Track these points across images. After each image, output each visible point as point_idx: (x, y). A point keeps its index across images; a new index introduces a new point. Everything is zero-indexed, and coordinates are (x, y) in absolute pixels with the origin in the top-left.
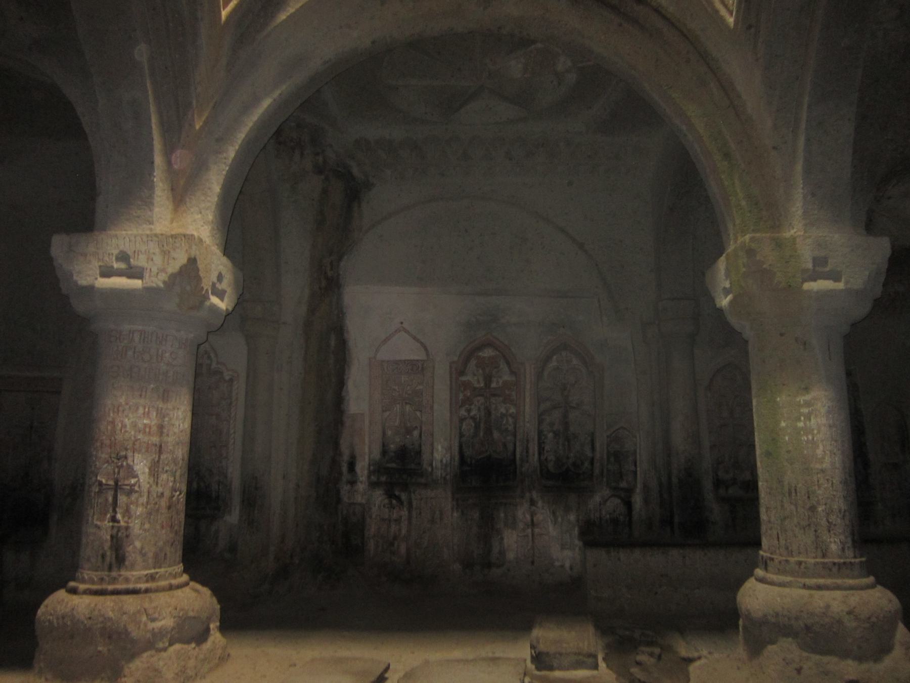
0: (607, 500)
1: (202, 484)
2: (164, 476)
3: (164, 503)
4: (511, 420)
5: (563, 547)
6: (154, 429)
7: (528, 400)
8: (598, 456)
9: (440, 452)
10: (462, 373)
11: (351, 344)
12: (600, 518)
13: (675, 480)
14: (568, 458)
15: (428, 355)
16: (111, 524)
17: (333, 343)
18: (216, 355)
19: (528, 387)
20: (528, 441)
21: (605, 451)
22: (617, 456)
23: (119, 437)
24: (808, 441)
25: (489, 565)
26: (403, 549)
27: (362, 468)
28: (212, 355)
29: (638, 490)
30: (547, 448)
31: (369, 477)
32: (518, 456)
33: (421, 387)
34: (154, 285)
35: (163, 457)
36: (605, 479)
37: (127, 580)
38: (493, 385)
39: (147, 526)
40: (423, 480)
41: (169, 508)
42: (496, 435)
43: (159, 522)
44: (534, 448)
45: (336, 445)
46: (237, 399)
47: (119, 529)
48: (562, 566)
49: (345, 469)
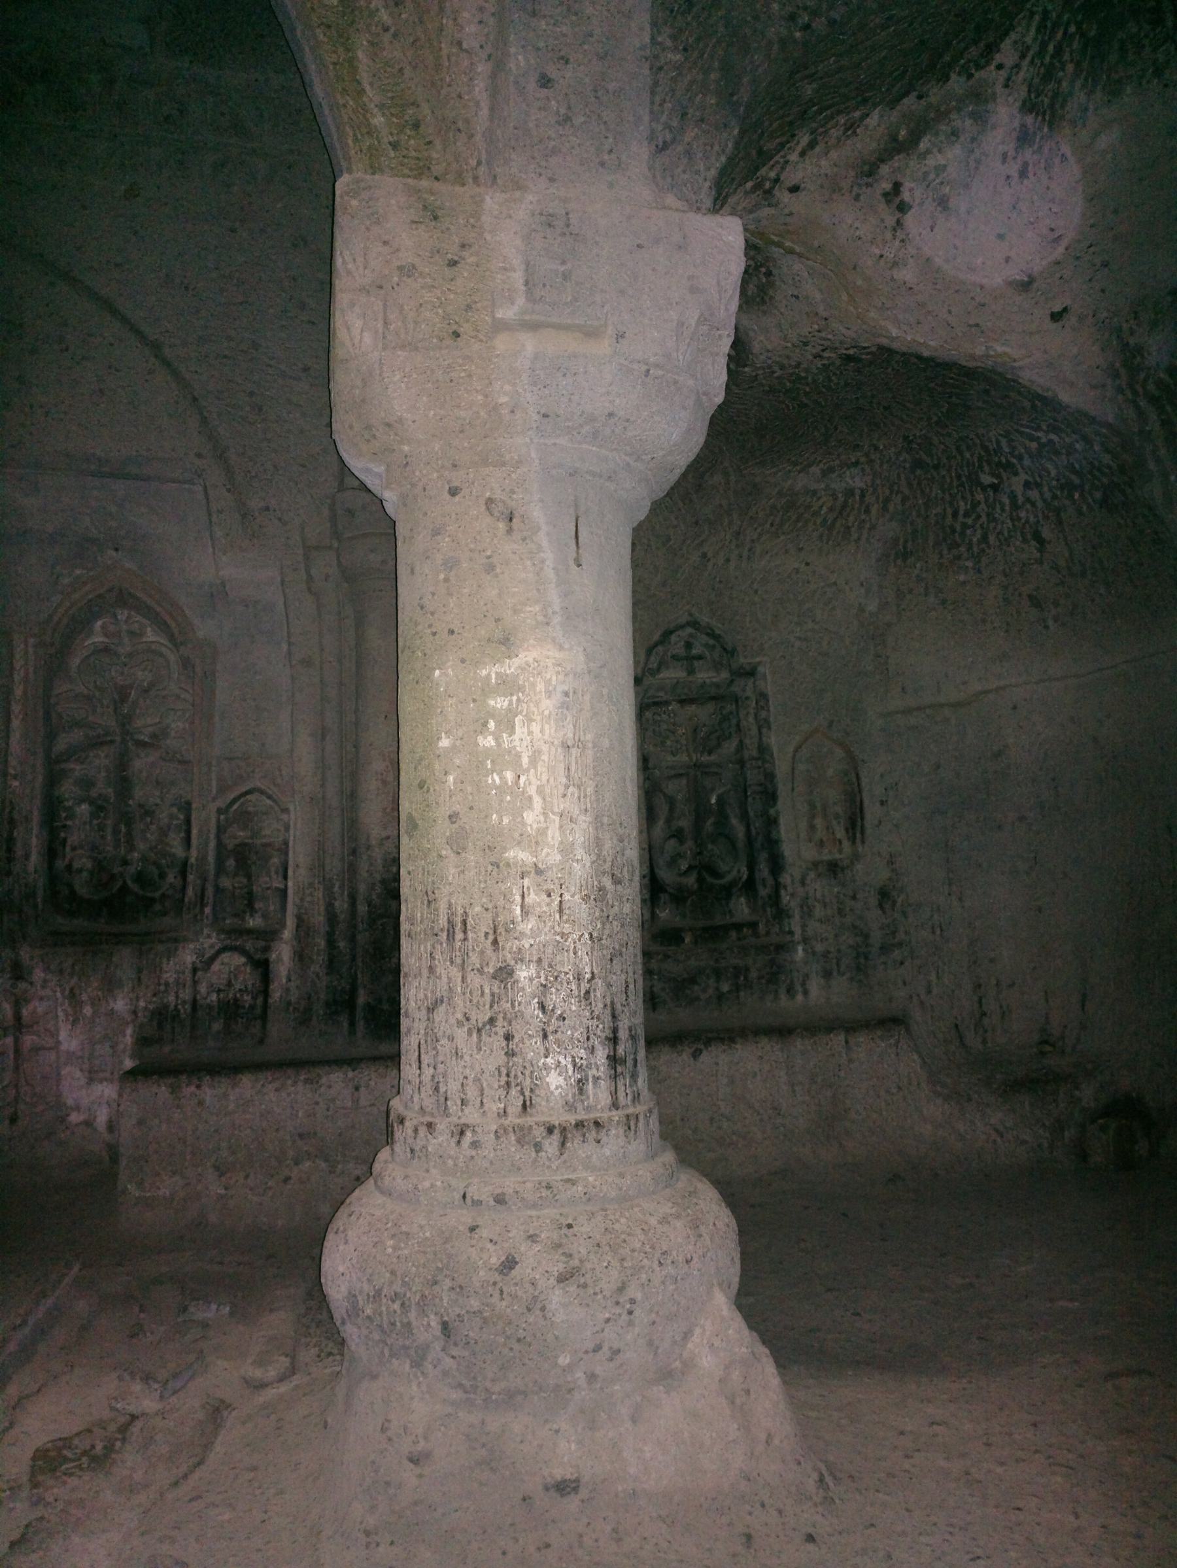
0: (213, 959)
5: (92, 1077)
7: (16, 723)
8: (194, 853)
12: (195, 1001)
13: (362, 908)
14: (125, 863)
19: (18, 692)
20: (12, 821)
21: (212, 844)
22: (243, 858)
24: (502, 789)
29: (287, 934)
30: (74, 839)
36: (207, 910)
48: (88, 1123)
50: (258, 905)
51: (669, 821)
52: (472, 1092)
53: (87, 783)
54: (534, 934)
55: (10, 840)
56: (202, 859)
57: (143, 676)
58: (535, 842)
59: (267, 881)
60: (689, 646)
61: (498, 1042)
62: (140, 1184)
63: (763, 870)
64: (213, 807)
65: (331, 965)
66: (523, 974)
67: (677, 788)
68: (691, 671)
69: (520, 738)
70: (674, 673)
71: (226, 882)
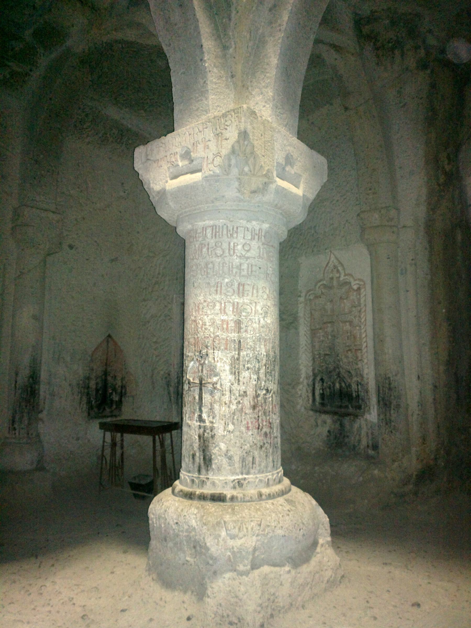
1: (343, 385)
2: (246, 374)
3: (247, 402)
6: (232, 324)
16: (198, 424)
18: (344, 269)
28: (340, 268)
34: (211, 173)
35: (243, 353)
37: (214, 484)
39: (231, 427)
41: (254, 407)
43: (244, 422)
46: (365, 305)
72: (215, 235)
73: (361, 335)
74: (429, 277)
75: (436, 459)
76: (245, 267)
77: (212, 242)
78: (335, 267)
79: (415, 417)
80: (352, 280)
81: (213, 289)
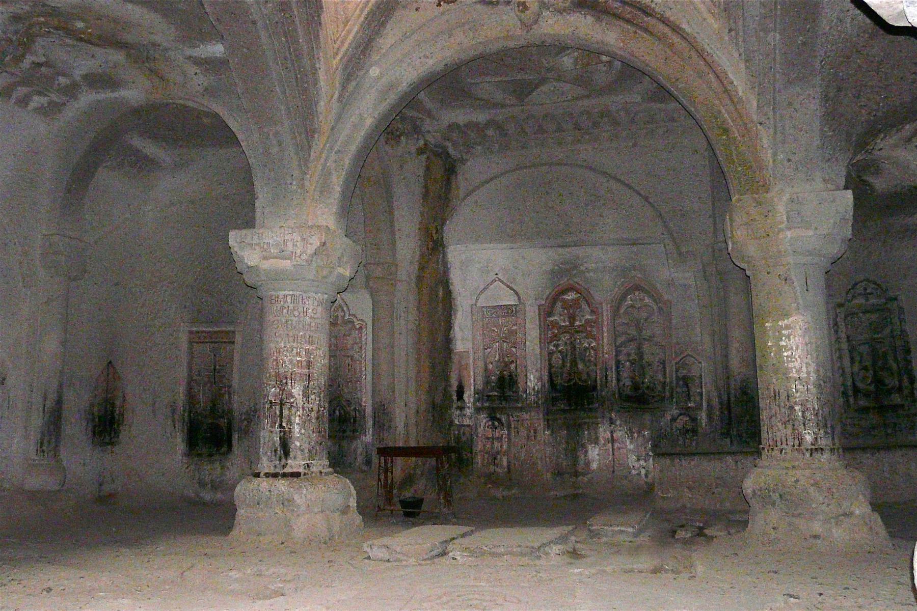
2: (313, 397)
3: (314, 414)
4: (592, 352)
6: (304, 364)
8: (668, 380)
9: (533, 380)
10: (550, 314)
11: (455, 294)
14: (643, 383)
15: (519, 298)
17: (441, 294)
22: (686, 381)
23: (282, 370)
24: (787, 357)
25: (576, 474)
26: (505, 463)
27: (469, 396)
28: (345, 309)
30: (625, 375)
31: (474, 404)
32: (599, 382)
33: (515, 328)
37: (291, 467)
38: (577, 323)
39: (303, 431)
40: (520, 405)
41: (317, 418)
42: (581, 366)
44: (612, 375)
45: (447, 379)
47: (285, 432)
48: (639, 474)
49: (455, 397)
50: (692, 398)
51: (861, 362)
52: (784, 440)
53: (629, 355)
54: (800, 396)
55: (606, 376)
56: (671, 382)
57: (645, 315)
58: (799, 371)
59: (695, 390)
60: (865, 289)
61: (790, 426)
62: (662, 493)
63: (906, 383)
64: (674, 362)
65: (722, 421)
66: (797, 408)
67: (864, 349)
68: (867, 300)
69: (793, 342)
70: (860, 301)
71: (679, 390)
72: (293, 302)
73: (361, 369)
74: (417, 323)
75: (415, 469)
76: (313, 324)
77: (291, 306)
78: (340, 306)
79: (402, 436)
80: (355, 319)
81: (291, 339)
